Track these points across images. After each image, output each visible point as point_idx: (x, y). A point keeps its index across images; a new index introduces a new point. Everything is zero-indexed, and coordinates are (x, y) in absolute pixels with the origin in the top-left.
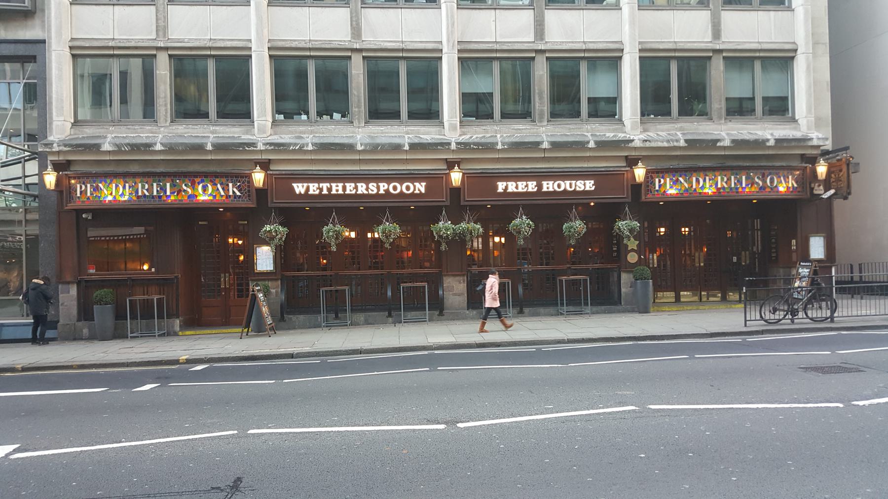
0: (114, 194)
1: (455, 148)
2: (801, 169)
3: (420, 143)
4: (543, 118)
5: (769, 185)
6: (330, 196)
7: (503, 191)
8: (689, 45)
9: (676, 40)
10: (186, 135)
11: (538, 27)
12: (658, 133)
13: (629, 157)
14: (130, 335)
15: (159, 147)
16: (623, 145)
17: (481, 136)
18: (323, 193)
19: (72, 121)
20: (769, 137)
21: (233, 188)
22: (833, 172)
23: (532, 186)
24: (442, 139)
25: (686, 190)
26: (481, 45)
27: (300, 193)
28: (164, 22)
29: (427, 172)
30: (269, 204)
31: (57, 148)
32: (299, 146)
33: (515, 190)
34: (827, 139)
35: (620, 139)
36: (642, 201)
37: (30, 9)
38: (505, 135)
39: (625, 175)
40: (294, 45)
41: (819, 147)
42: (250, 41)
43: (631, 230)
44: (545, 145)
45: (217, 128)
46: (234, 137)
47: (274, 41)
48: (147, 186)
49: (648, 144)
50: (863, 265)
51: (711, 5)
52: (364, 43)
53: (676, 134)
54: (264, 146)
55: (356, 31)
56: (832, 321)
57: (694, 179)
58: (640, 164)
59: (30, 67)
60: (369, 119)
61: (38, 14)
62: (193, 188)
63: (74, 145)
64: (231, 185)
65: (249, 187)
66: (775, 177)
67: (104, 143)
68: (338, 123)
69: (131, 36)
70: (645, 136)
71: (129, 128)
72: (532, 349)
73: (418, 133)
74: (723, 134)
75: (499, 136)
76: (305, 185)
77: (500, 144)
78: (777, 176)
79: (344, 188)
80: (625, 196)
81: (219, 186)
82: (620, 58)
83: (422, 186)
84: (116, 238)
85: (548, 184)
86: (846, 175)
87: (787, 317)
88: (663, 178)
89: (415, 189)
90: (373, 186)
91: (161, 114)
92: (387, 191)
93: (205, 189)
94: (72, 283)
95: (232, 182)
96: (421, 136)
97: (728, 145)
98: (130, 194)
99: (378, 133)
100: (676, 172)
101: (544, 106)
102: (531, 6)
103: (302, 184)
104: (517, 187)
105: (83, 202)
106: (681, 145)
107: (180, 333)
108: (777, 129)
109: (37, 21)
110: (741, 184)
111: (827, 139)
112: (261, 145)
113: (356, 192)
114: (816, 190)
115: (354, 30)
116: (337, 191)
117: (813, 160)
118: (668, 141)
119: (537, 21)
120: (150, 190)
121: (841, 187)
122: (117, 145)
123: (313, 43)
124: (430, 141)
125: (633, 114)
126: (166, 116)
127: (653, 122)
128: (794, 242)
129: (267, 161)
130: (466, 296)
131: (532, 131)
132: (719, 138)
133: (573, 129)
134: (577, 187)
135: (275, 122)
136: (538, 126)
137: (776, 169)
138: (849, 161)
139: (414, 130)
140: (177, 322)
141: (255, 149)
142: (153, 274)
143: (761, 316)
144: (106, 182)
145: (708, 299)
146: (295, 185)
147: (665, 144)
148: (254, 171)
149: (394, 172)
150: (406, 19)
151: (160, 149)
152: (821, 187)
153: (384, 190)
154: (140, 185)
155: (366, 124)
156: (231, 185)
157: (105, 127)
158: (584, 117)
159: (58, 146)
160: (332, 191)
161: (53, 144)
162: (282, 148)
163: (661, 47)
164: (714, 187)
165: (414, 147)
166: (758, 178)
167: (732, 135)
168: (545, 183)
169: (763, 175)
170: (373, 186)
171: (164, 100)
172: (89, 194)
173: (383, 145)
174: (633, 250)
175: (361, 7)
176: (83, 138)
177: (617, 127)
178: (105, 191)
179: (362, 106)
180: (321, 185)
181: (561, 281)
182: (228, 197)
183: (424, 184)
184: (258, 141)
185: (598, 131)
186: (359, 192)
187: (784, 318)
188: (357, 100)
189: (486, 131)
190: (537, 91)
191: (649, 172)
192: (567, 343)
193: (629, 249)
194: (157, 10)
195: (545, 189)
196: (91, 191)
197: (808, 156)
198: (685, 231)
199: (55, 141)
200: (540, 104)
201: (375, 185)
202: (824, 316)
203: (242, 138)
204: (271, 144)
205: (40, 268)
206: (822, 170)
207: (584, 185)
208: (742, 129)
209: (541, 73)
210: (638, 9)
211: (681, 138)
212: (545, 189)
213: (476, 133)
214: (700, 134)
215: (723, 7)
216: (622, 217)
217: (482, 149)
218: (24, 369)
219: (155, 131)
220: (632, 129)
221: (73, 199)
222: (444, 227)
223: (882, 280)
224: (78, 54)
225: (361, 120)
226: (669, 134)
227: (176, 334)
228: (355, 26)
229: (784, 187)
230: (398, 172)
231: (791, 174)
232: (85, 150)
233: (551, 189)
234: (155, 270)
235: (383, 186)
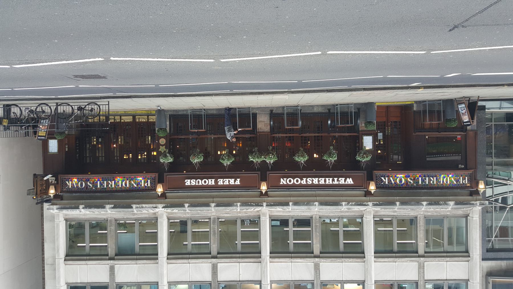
0: (448, 178)
1: (264, 203)
2: (63, 191)
3: (283, 206)
4: (213, 220)
5: (83, 182)
6: (333, 177)
7: (237, 179)
8: (129, 263)
9: (136, 265)
10: (410, 210)
11: (215, 271)
12: (148, 212)
13: (165, 198)
14: (441, 102)
15: (425, 203)
16: (169, 205)
17: (249, 210)
18: (337, 178)
19: (468, 217)
20: (83, 210)
22: (44, 190)
23: (221, 182)
24: (271, 208)
25: (132, 179)
26: (248, 261)
27: (349, 178)
28: (420, 271)
29: (279, 190)
30: (366, 173)
31: (477, 202)
33: (230, 180)
34: (48, 209)
35: (170, 208)
36: (158, 173)
37: (489, 277)
38: (235, 210)
39: (167, 188)
40: (351, 260)
41: (53, 204)
42: (375, 262)
43: (166, 156)
44: (213, 205)
45: (393, 214)
46: (384, 209)
47: (362, 261)
48: (431, 182)
49: (154, 205)
50: (24, 136)
51: (115, 285)
52: (313, 261)
53: (137, 212)
54: (368, 204)
55: (317, 268)
56: (57, 103)
57: (128, 186)
58: (160, 194)
59: (490, 245)
60: (310, 219)
61: (485, 274)
62: (407, 181)
63: (468, 204)
64: (387, 183)
65: (377, 182)
66: (80, 187)
67: (453, 205)
68: (327, 217)
69: (438, 263)
70: (155, 210)
71: (439, 213)
72: (235, 91)
73: (283, 212)
74: (109, 212)
75: (239, 210)
76: (346, 183)
77: (239, 205)
78: (78, 188)
79: (325, 181)
80: (168, 176)
81: (393, 182)
82: (168, 254)
83: (282, 182)
84: (447, 155)
85: (212, 183)
86: (38, 188)
87: (84, 106)
88: (146, 187)
89: (286, 180)
90: (309, 182)
91: (422, 221)
92: (302, 179)
93: (401, 181)
94: (469, 130)
95: (386, 184)
96: (282, 210)
97: (107, 205)
98: (440, 178)
99: (306, 211)
100: (138, 190)
101: (212, 227)
102: (219, 283)
103: (348, 183)
104: (229, 181)
105: (464, 174)
106: (135, 205)
107: (413, 103)
108: (77, 215)
109: (485, 271)
110: (100, 183)
111: (48, 209)
112: (370, 205)
113: (319, 179)
115: (318, 268)
116: (329, 180)
117: (56, 196)
118: (142, 207)
119: (216, 275)
121: (40, 181)
122: (447, 204)
123: (341, 261)
124: (278, 207)
125: (162, 223)
126: (420, 220)
127: (150, 218)
128: (67, 150)
129: (367, 196)
130: (257, 121)
131: (220, 213)
132: (112, 209)
133: (196, 214)
134: (195, 181)
135: (362, 217)
136: (216, 216)
137: (79, 191)
138: (36, 196)
139: (286, 213)
140: (415, 109)
141: (373, 203)
142: (427, 135)
143: (99, 107)
144: (452, 184)
145: (114, 117)
146: (352, 183)
147: (144, 205)
148: (375, 190)
149: (297, 190)
150: (290, 274)
151: (424, 202)
152: (50, 181)
153: (303, 180)
154: (435, 183)
155: (312, 216)
156: (387, 183)
157: (451, 214)
158: (189, 221)
159: (476, 204)
160: (332, 179)
161: (480, 205)
162: (359, 203)
163: (145, 261)
164: (116, 181)
165: (287, 204)
166: (90, 186)
167: (104, 211)
168: (213, 184)
169: (87, 188)
170: (309, 182)
171: (421, 229)
172: (461, 178)
173: (303, 205)
174: (162, 146)
176: (463, 208)
177: (171, 216)
178: (453, 179)
179: (314, 227)
180: (338, 183)
181: (205, 129)
182: (388, 177)
183: (281, 183)
184: (371, 207)
185: (182, 213)
186: (317, 179)
187: (86, 106)
188: (317, 230)
189: (245, 213)
190: (216, 235)
191: (154, 190)
192: (213, 94)
193: (165, 146)
194: (424, 278)
195: (213, 180)
196: (460, 180)
197: (60, 199)
198: (126, 156)
199: (478, 206)
200: (214, 228)
201: (308, 183)
202: (62, 107)
203: (380, 209)
204: (365, 205)
205: (486, 139)
206: (52, 191)
207: (191, 183)
208: (98, 214)
209: (214, 246)
210: (158, 282)
211: (134, 209)
212: (213, 180)
213: (251, 212)
214: (123, 212)
215: (108, 285)
216: (169, 164)
217: (249, 203)
218: (503, 85)
219: (426, 212)
220: (163, 214)
221: (469, 175)
222: (271, 160)
223: (15, 127)
224: (466, 253)
226: (141, 211)
227: (416, 102)
228: (318, 271)
229: (74, 181)
230: (296, 190)
231: (70, 188)
232: (463, 202)
233: (210, 180)
234: (426, 137)
235: (304, 182)
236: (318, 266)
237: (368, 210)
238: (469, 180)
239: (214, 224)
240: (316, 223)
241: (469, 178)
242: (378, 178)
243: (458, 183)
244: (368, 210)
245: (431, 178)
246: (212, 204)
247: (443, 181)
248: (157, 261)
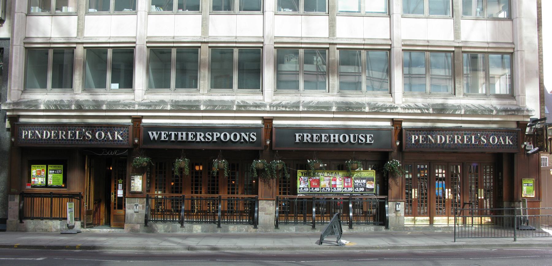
2: (515, 132)
5: (492, 143)
21: (117, 135)
48: (64, 133)
70: (406, 106)
81: (109, 134)
91: (77, 86)
94: (17, 194)
95: (117, 131)
114: (528, 147)
120: (66, 136)
169: (487, 136)
175: (209, 14)
194: (79, 19)
238: (20, 134)
241: (20, 137)
247: (51, 133)
248: (403, 42)
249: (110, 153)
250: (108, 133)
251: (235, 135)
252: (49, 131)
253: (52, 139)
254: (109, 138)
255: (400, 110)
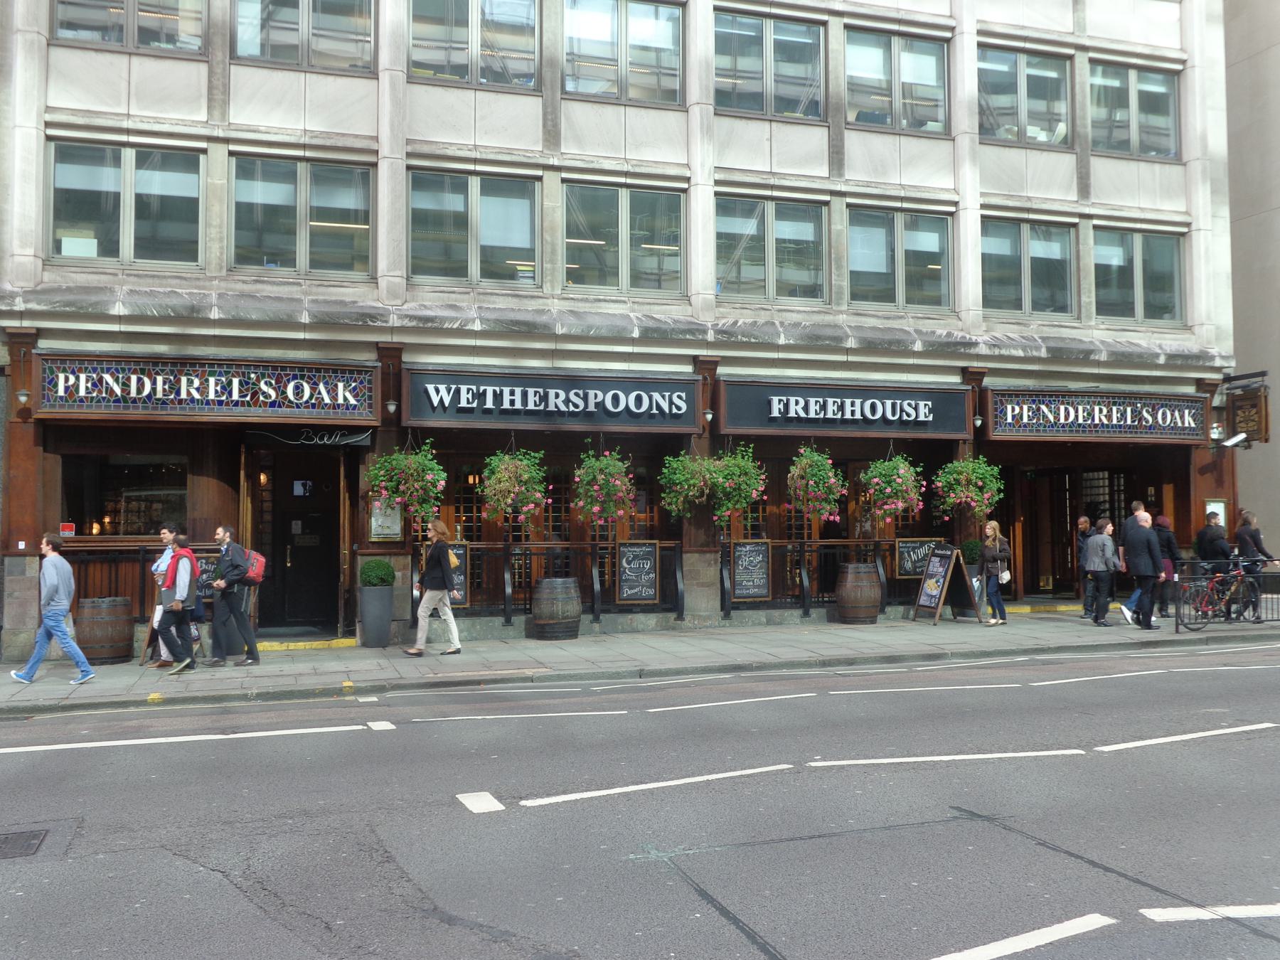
32: (459, 322)
42: (376, 139)
48: (197, 382)
52: (565, 157)
64: (341, 385)
81: (322, 387)
95: (343, 381)
112: (395, 317)
119: (833, 146)
132: (1092, 348)
141: (384, 325)
156: (341, 385)
171: (218, 230)
182: (335, 406)
188: (550, 250)
194: (211, 73)
197: (1207, 382)
200: (838, 276)
209: (839, 227)
225: (556, 284)
228: (550, 128)
236: (549, 141)
237: (399, 302)
239: (840, 287)
240: (554, 270)
242: (365, 400)
243: (94, 376)
244: (399, 302)
245: (197, 396)
246: (853, 346)
247: (154, 383)
249: (321, 439)
250: (318, 385)
251: (638, 399)
252: (149, 376)
253: (159, 399)
254: (323, 399)
255: (983, 350)
